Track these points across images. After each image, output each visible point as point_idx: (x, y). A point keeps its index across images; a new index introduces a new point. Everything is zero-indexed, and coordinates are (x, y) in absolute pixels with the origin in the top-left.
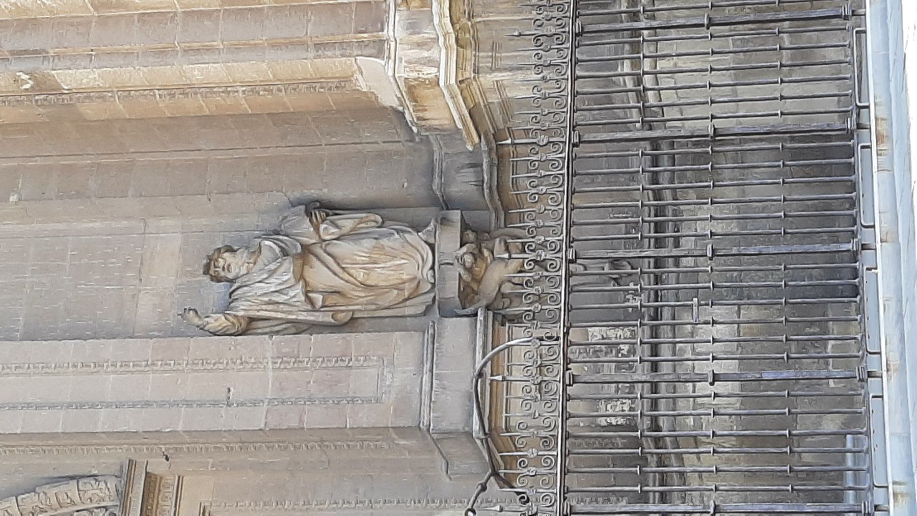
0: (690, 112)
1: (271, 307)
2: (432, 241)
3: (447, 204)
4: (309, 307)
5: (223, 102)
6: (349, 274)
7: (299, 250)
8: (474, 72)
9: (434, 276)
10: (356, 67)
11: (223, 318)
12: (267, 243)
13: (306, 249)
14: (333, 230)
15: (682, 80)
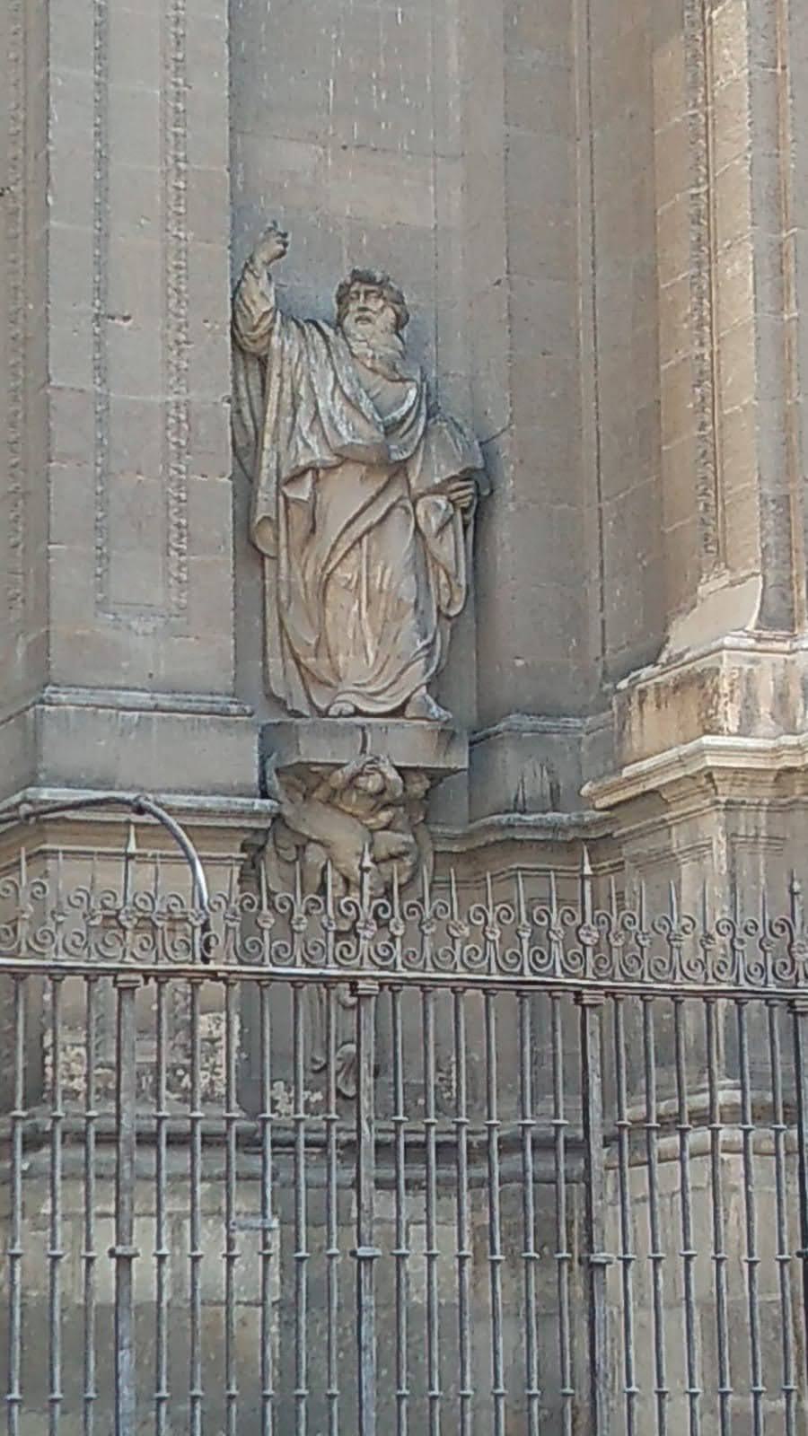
0: (640, 1218)
1: (287, 399)
2: (410, 712)
3: (481, 742)
4: (285, 474)
5: (681, 316)
6: (348, 552)
7: (396, 457)
8: (728, 802)
9: (340, 715)
10: (743, 574)
11: (267, 308)
12: (413, 393)
13: (401, 468)
14: (435, 522)
15: (701, 1204)
